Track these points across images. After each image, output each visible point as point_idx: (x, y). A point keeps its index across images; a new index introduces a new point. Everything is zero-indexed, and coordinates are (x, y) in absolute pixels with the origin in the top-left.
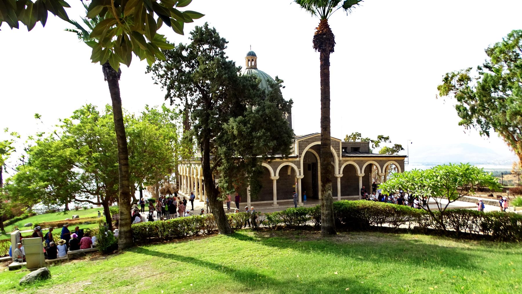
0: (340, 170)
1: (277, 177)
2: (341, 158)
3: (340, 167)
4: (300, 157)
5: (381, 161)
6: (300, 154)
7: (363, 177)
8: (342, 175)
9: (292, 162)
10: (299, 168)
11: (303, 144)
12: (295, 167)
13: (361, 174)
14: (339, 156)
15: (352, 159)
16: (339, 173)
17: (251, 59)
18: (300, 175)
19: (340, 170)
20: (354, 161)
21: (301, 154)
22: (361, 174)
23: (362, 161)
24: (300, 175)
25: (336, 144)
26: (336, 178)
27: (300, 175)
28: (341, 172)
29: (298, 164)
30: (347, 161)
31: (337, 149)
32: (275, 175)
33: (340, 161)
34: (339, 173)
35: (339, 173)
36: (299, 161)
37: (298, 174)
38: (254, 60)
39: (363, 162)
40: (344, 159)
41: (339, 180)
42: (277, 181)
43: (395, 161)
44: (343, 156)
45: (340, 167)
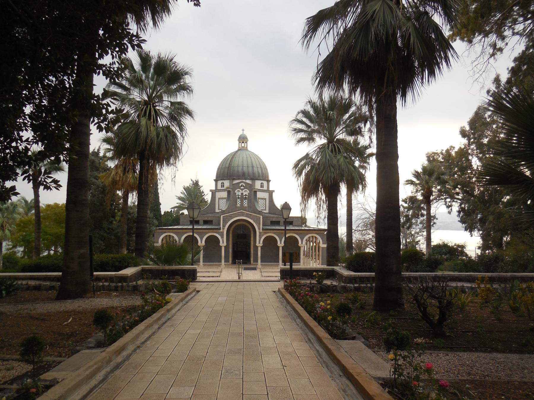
0: (260, 240)
2: (261, 231)
3: (260, 238)
4: (223, 229)
5: (301, 233)
6: (224, 226)
8: (261, 245)
10: (222, 237)
12: (219, 237)
13: (281, 243)
14: (259, 229)
15: (272, 231)
16: (259, 243)
17: (241, 142)
19: (260, 240)
20: (274, 233)
24: (223, 243)
26: (257, 247)
27: (223, 243)
29: (222, 235)
30: (268, 233)
33: (260, 233)
34: (259, 243)
35: (259, 243)
36: (223, 232)
37: (221, 242)
38: (245, 142)
41: (259, 249)
43: (316, 233)
44: (263, 229)
45: (260, 238)
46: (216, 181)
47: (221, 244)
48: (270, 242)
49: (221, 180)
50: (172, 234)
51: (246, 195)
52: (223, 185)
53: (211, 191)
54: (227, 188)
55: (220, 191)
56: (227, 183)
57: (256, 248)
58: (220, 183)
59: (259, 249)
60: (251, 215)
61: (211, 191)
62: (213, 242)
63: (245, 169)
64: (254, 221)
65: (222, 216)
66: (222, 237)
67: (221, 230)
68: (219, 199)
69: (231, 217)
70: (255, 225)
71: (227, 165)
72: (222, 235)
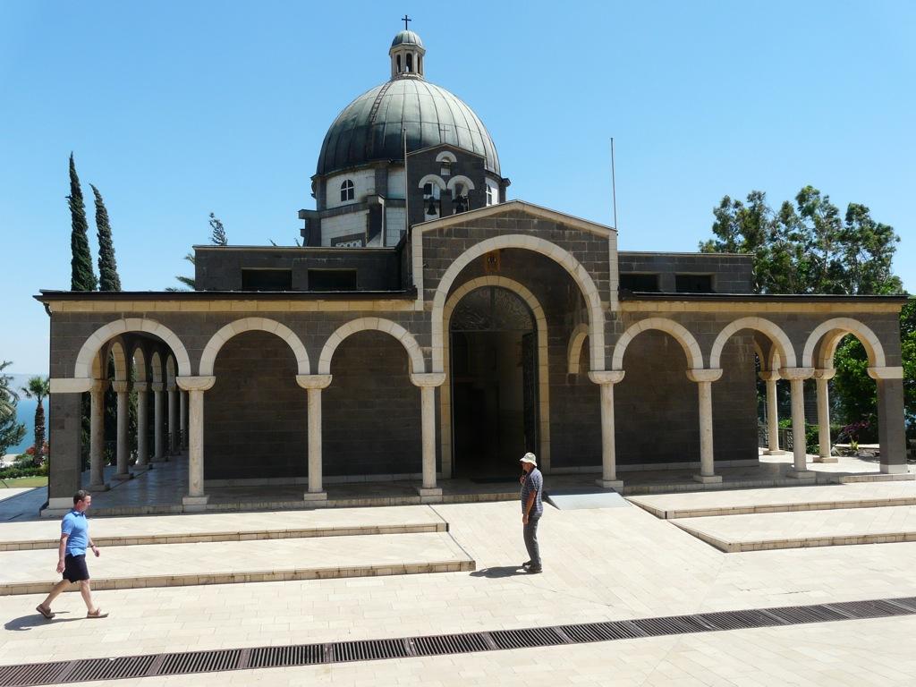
0: (609, 353)
1: (325, 380)
2: (615, 306)
3: (611, 342)
4: (429, 297)
6: (431, 283)
7: (713, 384)
8: (618, 377)
9: (393, 317)
10: (424, 340)
13: (705, 372)
14: (605, 296)
15: (664, 306)
16: (608, 368)
18: (430, 374)
19: (609, 353)
20: (676, 317)
21: (436, 284)
22: (705, 372)
23: (710, 317)
24: (429, 370)
27: (429, 370)
28: (618, 361)
29: (420, 325)
30: (646, 315)
31: (597, 268)
32: (314, 371)
33: (609, 316)
36: (426, 316)
39: (719, 323)
40: (631, 307)
41: (608, 396)
45: (611, 342)
46: (319, 184)
47: (416, 380)
48: (655, 367)
49: (345, 172)
52: (347, 193)
53: (304, 214)
54: (365, 199)
55: (338, 212)
56: (363, 182)
58: (335, 185)
59: (608, 396)
61: (304, 214)
62: (373, 362)
64: (579, 257)
66: (424, 340)
67: (419, 305)
72: (420, 325)
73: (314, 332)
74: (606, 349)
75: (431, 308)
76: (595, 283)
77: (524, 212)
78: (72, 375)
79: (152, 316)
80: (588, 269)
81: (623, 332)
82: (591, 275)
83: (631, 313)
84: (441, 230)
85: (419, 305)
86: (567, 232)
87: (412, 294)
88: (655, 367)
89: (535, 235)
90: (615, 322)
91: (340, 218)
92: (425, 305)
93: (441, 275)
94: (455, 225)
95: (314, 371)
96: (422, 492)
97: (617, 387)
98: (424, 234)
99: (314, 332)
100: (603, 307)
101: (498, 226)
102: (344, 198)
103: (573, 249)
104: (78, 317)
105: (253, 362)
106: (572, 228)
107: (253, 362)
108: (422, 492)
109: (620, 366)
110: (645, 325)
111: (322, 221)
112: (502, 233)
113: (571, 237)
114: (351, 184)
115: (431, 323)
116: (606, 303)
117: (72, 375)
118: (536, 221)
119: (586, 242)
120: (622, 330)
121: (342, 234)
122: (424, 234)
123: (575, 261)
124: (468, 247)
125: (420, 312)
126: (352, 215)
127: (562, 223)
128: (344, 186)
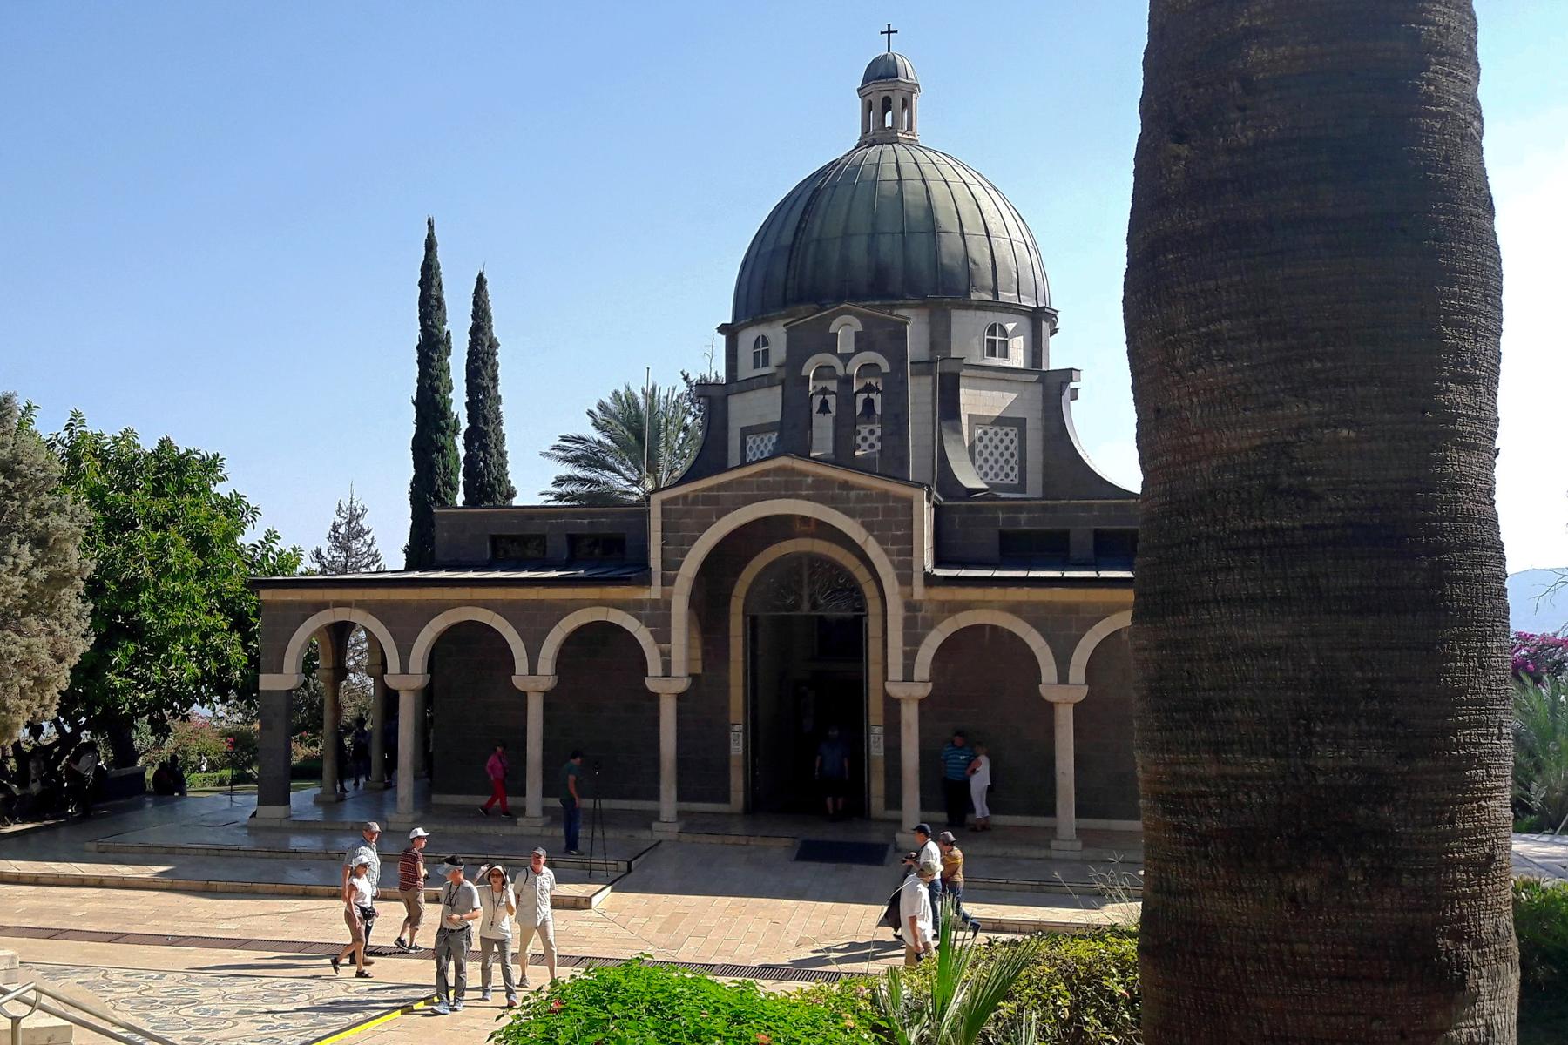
0: (910, 658)
2: (919, 592)
3: (913, 641)
4: (668, 581)
9: (623, 606)
10: (662, 635)
11: (687, 514)
12: (643, 635)
14: (905, 580)
15: (994, 593)
16: (908, 677)
19: (910, 658)
21: (678, 566)
24: (667, 672)
25: (888, 512)
27: (667, 672)
28: (923, 668)
32: (533, 670)
33: (911, 607)
34: (908, 677)
41: (910, 715)
42: (549, 699)
45: (913, 641)
47: (652, 684)
49: (755, 322)
50: (357, 616)
51: (868, 389)
55: (751, 385)
57: (892, 706)
58: (747, 337)
59: (910, 715)
60: (846, 485)
63: (888, 247)
64: (869, 527)
65: (656, 500)
66: (662, 635)
67: (654, 592)
68: (746, 432)
69: (718, 505)
70: (873, 550)
71: (787, 238)
73: (534, 621)
74: (905, 653)
75: (671, 596)
76: (892, 562)
77: (793, 469)
78: (279, 669)
79: (360, 605)
80: (881, 541)
81: (931, 627)
82: (886, 551)
83: (943, 603)
84: (685, 497)
85: (654, 592)
86: (853, 494)
87: (646, 581)
88: (982, 676)
89: (808, 498)
90: (920, 615)
91: (750, 395)
92: (663, 593)
93: (684, 554)
94: (704, 490)
95: (533, 670)
96: (655, 825)
97: (922, 702)
98: (664, 503)
99: (534, 621)
100: (901, 593)
101: (759, 488)
102: (756, 366)
103: (861, 516)
104: (287, 605)
105: (469, 657)
106: (862, 488)
107: (469, 657)
108: (655, 825)
109: (927, 677)
110: (966, 619)
111: (731, 399)
112: (764, 498)
113: (859, 500)
114: (766, 342)
115: (670, 615)
116: (907, 589)
117: (279, 669)
118: (810, 480)
119: (880, 506)
120: (930, 625)
121: (754, 422)
122: (664, 503)
123: (863, 531)
124: (719, 518)
125: (656, 600)
126: (761, 393)
127: (846, 482)
128: (756, 345)
